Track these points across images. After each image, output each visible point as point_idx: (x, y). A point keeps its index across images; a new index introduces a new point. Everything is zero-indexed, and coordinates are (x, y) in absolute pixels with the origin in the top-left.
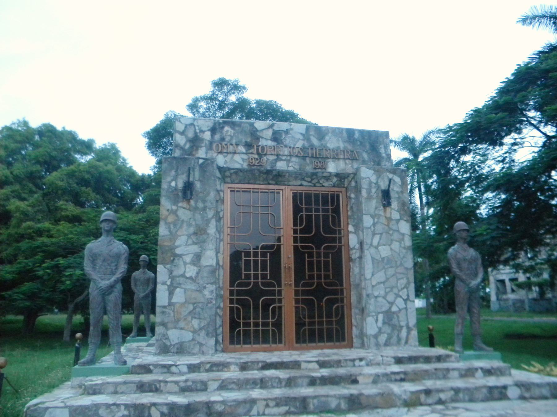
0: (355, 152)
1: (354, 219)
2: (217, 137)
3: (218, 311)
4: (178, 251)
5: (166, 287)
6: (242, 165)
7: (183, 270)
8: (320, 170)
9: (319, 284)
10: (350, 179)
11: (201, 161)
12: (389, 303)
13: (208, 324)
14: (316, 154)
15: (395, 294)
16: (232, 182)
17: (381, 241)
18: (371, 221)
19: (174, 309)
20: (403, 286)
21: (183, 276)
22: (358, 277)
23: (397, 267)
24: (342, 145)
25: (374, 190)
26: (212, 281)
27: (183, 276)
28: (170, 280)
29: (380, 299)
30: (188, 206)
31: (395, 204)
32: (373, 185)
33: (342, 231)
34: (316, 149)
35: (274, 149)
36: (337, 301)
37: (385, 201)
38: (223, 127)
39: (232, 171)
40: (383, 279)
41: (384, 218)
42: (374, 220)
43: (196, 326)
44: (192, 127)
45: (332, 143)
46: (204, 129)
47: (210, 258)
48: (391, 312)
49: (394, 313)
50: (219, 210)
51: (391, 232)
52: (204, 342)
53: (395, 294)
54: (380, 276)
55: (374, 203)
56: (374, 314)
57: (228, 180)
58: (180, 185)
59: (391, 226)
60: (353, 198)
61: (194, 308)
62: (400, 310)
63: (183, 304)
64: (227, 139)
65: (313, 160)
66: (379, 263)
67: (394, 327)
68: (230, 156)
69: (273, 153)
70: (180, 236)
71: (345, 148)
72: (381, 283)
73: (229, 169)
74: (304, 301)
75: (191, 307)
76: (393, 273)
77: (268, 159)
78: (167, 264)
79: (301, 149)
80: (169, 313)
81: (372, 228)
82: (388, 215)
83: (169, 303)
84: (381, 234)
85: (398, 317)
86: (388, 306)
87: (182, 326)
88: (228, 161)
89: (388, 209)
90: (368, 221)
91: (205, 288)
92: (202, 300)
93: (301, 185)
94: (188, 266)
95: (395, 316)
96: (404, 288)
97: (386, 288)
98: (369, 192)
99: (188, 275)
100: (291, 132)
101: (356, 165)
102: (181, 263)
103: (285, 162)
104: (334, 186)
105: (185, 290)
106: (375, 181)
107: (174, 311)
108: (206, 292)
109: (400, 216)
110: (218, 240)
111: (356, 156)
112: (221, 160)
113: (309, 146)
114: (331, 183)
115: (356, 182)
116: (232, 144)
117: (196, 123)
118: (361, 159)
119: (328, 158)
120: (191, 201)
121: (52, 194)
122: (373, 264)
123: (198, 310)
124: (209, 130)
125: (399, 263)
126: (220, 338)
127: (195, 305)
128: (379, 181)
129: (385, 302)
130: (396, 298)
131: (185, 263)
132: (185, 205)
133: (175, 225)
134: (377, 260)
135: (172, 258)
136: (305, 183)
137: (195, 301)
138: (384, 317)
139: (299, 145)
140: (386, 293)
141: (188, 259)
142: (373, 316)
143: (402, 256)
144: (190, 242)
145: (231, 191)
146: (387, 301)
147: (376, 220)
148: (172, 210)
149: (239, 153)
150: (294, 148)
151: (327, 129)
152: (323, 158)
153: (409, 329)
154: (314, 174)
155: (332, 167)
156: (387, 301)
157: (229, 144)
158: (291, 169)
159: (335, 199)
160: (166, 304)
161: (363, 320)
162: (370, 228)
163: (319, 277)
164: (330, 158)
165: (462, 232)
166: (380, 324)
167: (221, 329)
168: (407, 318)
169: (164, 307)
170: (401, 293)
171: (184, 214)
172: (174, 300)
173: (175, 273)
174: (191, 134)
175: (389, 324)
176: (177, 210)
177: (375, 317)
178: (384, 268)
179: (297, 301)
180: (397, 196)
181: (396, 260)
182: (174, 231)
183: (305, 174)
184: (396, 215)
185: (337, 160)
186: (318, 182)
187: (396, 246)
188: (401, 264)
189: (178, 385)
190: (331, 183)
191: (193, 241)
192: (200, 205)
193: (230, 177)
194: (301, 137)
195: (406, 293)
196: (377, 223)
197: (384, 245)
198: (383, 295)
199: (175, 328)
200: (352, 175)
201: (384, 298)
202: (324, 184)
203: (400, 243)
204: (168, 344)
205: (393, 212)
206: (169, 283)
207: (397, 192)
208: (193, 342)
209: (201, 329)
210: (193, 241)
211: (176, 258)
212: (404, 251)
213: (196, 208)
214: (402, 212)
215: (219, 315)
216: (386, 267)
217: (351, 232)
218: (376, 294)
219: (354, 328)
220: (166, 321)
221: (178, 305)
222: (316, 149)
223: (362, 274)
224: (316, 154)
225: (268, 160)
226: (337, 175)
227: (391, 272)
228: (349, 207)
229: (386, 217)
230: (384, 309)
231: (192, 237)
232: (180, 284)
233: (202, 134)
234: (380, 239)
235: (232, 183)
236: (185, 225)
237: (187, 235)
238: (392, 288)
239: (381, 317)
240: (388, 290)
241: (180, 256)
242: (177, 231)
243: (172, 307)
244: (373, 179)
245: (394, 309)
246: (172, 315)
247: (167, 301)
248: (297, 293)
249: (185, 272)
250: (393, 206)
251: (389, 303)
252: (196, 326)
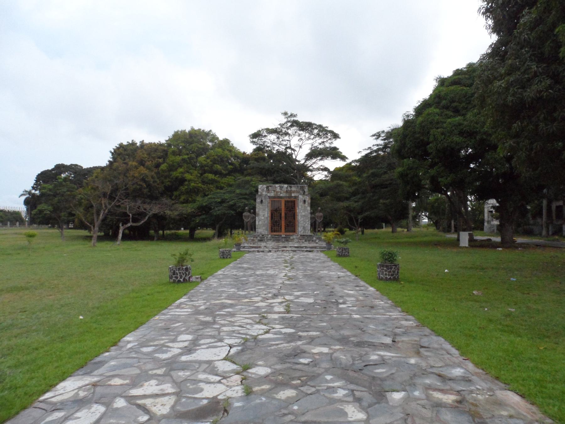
31: (307, 203)
47: (266, 216)
54: (302, 219)
66: (302, 216)
90: (300, 207)
112: (269, 195)
121: (204, 170)
155: (293, 195)
159: (295, 201)
171: (261, 207)
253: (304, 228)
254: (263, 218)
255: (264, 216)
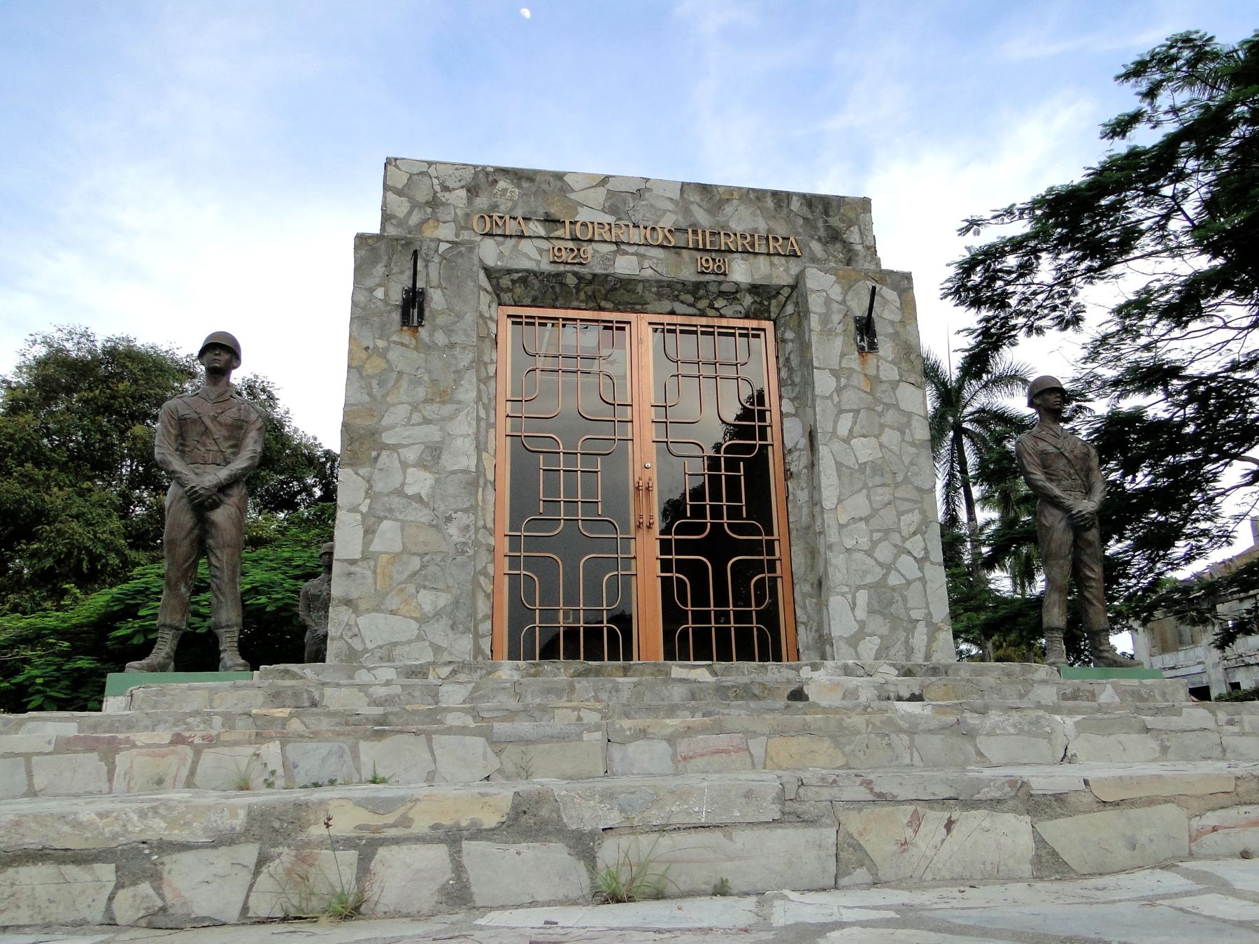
0: (792, 239)
1: (793, 384)
2: (482, 202)
3: (482, 579)
4: (388, 438)
5: (359, 517)
6: (538, 262)
7: (400, 480)
8: (713, 277)
9: (717, 528)
10: (782, 298)
11: (443, 247)
12: (881, 565)
13: (456, 602)
14: (704, 244)
15: (896, 546)
16: (516, 304)
17: (857, 428)
18: (832, 383)
19: (375, 566)
20: (912, 529)
21: (399, 492)
22: (805, 511)
23: (897, 485)
24: (762, 226)
25: (836, 318)
26: (467, 505)
27: (399, 492)
28: (368, 501)
29: (858, 556)
30: (414, 342)
31: (886, 348)
32: (835, 306)
33: (768, 414)
34: (704, 231)
35: (610, 230)
36: (757, 567)
37: (862, 340)
38: (496, 181)
39: (516, 276)
40: (865, 512)
41: (862, 377)
42: (838, 380)
43: (427, 608)
44: (426, 180)
45: (742, 220)
46: (451, 184)
48: (885, 586)
49: (893, 589)
50: (487, 359)
51: (879, 409)
52: (444, 645)
53: (896, 546)
54: (859, 504)
55: (838, 342)
56: (846, 589)
57: (506, 297)
58: (397, 297)
59: (878, 395)
60: (792, 341)
61: (423, 567)
62: (909, 583)
63: (395, 557)
64: (502, 208)
65: (698, 255)
67: (895, 621)
68: (511, 242)
69: (607, 237)
70: (394, 405)
71: (769, 231)
72: (861, 519)
73: (509, 271)
74: (681, 566)
75: (416, 563)
76: (887, 498)
77: (596, 251)
78: (362, 465)
79: (670, 231)
80: (364, 578)
81: (836, 399)
82: (871, 371)
83: (363, 552)
84: (857, 412)
85: (905, 600)
86: (878, 573)
87: (394, 607)
88: (507, 253)
89: (871, 358)
91: (449, 519)
92: (444, 548)
93: (672, 313)
94: (411, 470)
95: (897, 597)
96: (914, 534)
97: (872, 532)
98: (825, 319)
99: (410, 491)
100: (647, 195)
101: (795, 267)
102: (397, 464)
103: (635, 258)
104: (747, 317)
105: (404, 525)
106: (839, 298)
107: (375, 572)
108: (453, 530)
109: (901, 376)
110: (483, 424)
111: (796, 248)
113: (690, 226)
114: (739, 308)
115: (797, 304)
116: (515, 219)
117: (432, 171)
118: (806, 253)
119: (731, 251)
120: (420, 329)
122: (839, 477)
123: (432, 569)
124: (462, 187)
125: (899, 478)
126: (485, 644)
127: (427, 558)
128: (848, 298)
129: (873, 562)
130: (897, 557)
131: (404, 465)
132: (406, 337)
133: (381, 384)
134: (848, 467)
135: (374, 454)
136: (679, 307)
137: (426, 550)
138: (870, 597)
139: (668, 222)
140: (874, 544)
141: (411, 455)
142: (843, 595)
143: (907, 462)
144: (416, 417)
145: (513, 323)
146: (876, 560)
147: (843, 381)
148: (376, 347)
149: (530, 237)
150: (653, 229)
151: (731, 190)
152: (719, 251)
153: (933, 629)
154: (698, 286)
155: (740, 272)
156: (876, 560)
157: (507, 217)
158: (648, 273)
160: (358, 556)
161: (822, 605)
162: (830, 397)
163: (716, 512)
164: (737, 252)
165: (1047, 397)
166: (861, 613)
167: (488, 625)
168: (927, 603)
169: (353, 562)
170: (908, 545)
172: (376, 546)
173: (379, 486)
174: (422, 195)
175: (883, 615)
176: (387, 349)
177: (849, 597)
178: (865, 486)
179: (666, 566)
180: (891, 330)
181: (895, 469)
182: (379, 396)
183: (679, 287)
184: (889, 372)
185: (751, 257)
186: (711, 306)
187: (890, 437)
188: (906, 480)
189: (366, 694)
190: (739, 308)
191: (424, 417)
192: (440, 338)
193: (509, 290)
194: (670, 206)
195: (922, 545)
196: (844, 388)
197: (865, 436)
198: (866, 548)
199: (377, 609)
200: (786, 292)
201: (869, 553)
202: (722, 312)
203: (903, 433)
204: (359, 647)
205: (884, 366)
206: (364, 509)
207: (892, 323)
208: (421, 644)
209: (438, 615)
210: (424, 417)
211: (384, 453)
212: (913, 450)
213: (429, 348)
214: (904, 366)
215: (484, 591)
216: (870, 484)
217: (788, 415)
218: (849, 543)
219: (801, 629)
220: (354, 594)
221: (384, 559)
222: (704, 231)
223: (815, 503)
224: (704, 244)
225: (596, 258)
226: (754, 289)
227: (882, 495)
228: (781, 360)
229: (866, 375)
230: (869, 579)
231: (421, 406)
232: (391, 510)
233: (447, 195)
234: (855, 423)
235: (516, 305)
236: (404, 383)
237: (410, 404)
238: (887, 532)
239: (862, 597)
240: (876, 536)
241: (394, 448)
242: (388, 394)
243: (372, 563)
244: (836, 292)
245: (894, 580)
246: (370, 580)
247: (360, 548)
248: (665, 547)
249: (403, 484)
250: (881, 353)
251: (881, 565)
252: (427, 608)
253: (884, 599)
254: (420, 482)
255: (432, 455)
